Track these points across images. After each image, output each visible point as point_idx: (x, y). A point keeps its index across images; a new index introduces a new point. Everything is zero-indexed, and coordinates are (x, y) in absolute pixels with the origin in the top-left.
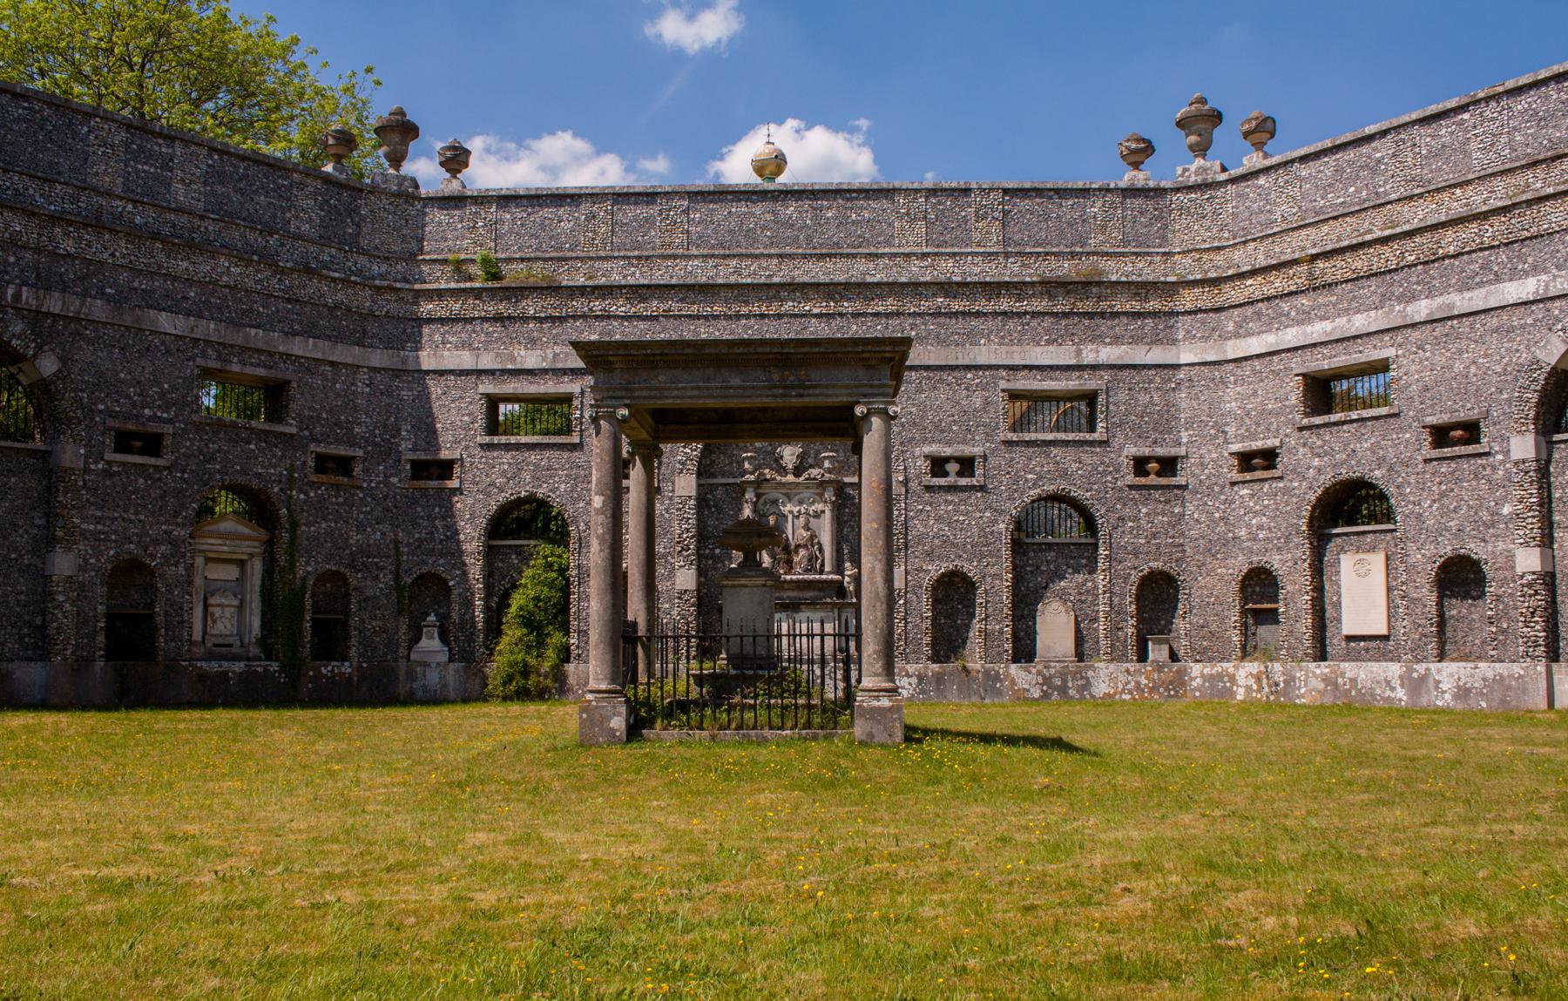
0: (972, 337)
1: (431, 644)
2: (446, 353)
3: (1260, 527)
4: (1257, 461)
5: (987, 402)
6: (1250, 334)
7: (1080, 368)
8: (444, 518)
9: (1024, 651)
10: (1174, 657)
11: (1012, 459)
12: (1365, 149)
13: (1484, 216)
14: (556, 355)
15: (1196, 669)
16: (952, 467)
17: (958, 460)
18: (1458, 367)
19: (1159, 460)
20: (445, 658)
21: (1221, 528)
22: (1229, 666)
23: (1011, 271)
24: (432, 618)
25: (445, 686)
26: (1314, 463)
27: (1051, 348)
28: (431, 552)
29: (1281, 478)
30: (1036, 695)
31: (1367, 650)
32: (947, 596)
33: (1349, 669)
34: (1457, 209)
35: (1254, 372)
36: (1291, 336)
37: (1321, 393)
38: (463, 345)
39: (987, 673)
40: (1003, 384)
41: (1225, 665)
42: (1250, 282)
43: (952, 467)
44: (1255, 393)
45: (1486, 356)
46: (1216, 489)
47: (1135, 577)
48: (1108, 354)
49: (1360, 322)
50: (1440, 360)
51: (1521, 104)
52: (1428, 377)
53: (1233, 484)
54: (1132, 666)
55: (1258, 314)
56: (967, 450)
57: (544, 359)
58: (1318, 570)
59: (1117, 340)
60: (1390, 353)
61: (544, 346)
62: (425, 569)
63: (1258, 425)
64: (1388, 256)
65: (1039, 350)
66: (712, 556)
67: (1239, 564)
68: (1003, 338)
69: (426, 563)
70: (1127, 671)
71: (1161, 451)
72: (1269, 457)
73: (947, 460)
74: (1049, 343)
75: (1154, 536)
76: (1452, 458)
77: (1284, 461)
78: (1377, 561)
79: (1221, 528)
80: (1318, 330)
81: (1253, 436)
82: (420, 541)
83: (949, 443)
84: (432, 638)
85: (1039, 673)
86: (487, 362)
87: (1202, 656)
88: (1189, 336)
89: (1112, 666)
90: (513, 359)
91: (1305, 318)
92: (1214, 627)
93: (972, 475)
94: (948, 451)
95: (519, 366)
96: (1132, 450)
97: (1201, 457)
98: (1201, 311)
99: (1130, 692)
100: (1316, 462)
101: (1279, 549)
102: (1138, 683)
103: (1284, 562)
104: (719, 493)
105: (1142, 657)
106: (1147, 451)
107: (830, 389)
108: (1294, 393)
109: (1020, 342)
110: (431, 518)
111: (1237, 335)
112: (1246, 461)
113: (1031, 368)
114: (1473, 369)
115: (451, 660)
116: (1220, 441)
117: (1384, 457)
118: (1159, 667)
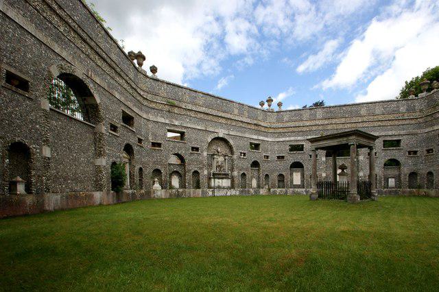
0: (245, 132)
4: (281, 158)
23: (249, 121)
26: (292, 158)
33: (296, 190)
34: (314, 124)
36: (287, 139)
38: (162, 117)
48: (261, 138)
49: (299, 138)
58: (291, 174)
64: (304, 129)
67: (277, 174)
72: (283, 157)
78: (299, 174)
80: (292, 138)
86: (167, 122)
91: (290, 136)
108: (288, 148)
112: (278, 157)
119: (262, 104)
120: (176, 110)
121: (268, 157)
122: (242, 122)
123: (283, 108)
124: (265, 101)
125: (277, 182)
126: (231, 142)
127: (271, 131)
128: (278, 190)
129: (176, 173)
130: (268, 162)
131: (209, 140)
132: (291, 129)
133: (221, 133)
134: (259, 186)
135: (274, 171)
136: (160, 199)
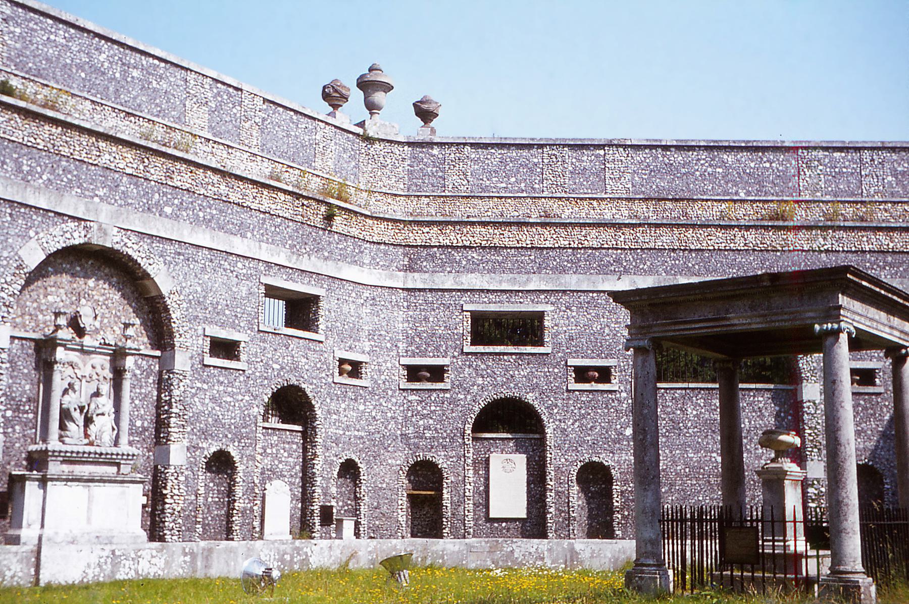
0: (241, 230)
6: (420, 271)
11: (265, 348)
12: (525, 153)
13: (618, 226)
18: (596, 327)
21: (392, 426)
31: (508, 530)
34: (594, 217)
37: (492, 329)
44: (426, 319)
45: (617, 323)
46: (390, 393)
50: (583, 321)
51: (640, 156)
52: (574, 330)
55: (433, 256)
60: (548, 308)
63: (428, 345)
64: (547, 238)
67: (400, 458)
72: (437, 373)
76: (590, 391)
77: (449, 376)
81: (423, 354)
88: (374, 264)
92: (384, 509)
100: (480, 381)
101: (444, 447)
107: (783, 315)
112: (414, 373)
114: (607, 331)
116: (394, 353)
117: (537, 385)
121: (355, 369)
122: (223, 174)
123: (444, 128)
124: (350, 83)
126: (163, 279)
130: (360, 394)
131: (33, 257)
132: (479, 236)
133: (110, 224)
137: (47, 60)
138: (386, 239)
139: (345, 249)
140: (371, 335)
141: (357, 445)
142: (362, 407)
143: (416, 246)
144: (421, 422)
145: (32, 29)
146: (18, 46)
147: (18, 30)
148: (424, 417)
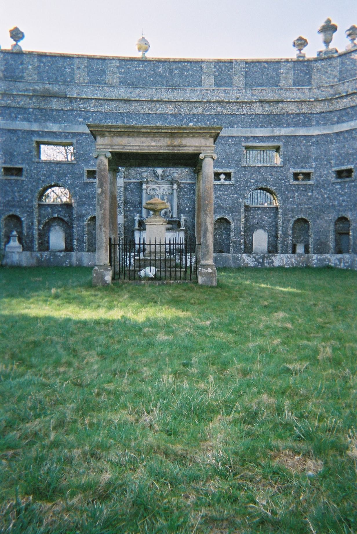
1: (14, 243)
2: (18, 122)
3: (343, 201)
5: (236, 151)
6: (343, 122)
7: (273, 137)
8: (19, 192)
9: (248, 250)
10: (307, 251)
14: (65, 127)
15: (315, 256)
16: (223, 177)
17: (225, 174)
19: (303, 174)
20: (21, 250)
21: (327, 201)
22: (328, 256)
24: (15, 233)
25: (21, 261)
27: (262, 129)
28: (13, 206)
29: (353, 181)
30: (252, 266)
32: (219, 227)
35: (344, 137)
39: (234, 257)
40: (243, 144)
41: (326, 255)
42: (345, 100)
43: (223, 177)
44: (344, 147)
47: (292, 220)
53: (333, 183)
54: (289, 255)
55: (348, 114)
56: (228, 171)
57: (60, 128)
59: (288, 125)
61: (60, 122)
62: (11, 213)
63: (344, 159)
65: (257, 129)
66: (129, 210)
68: (244, 125)
69: (11, 211)
70: (288, 257)
71: (304, 171)
73: (220, 174)
74: (262, 127)
75: (300, 204)
79: (327, 201)
81: (342, 164)
82: (9, 201)
83: (221, 167)
84: (14, 241)
85: (254, 257)
86: (35, 127)
87: (318, 251)
88: (318, 124)
89: (282, 255)
90: (47, 128)
93: (230, 180)
94: (221, 171)
95: (49, 130)
96: (292, 171)
97: (320, 173)
98: (323, 112)
99: (288, 265)
102: (292, 262)
103: (352, 215)
104: (132, 185)
105: (294, 252)
106: (298, 171)
109: (250, 127)
110: (13, 192)
111: (338, 122)
112: (340, 174)
113: (254, 137)
115: (23, 250)
116: (329, 166)
118: (300, 255)
119: (301, 43)
120: (55, 104)
121: (307, 176)
125: (332, 237)
127: (318, 108)
128: (332, 259)
129: (59, 219)
134: (273, 249)
135: (323, 209)
136: (17, 268)
137: (135, 78)
138: (324, 110)
139: (299, 120)
140: (316, 160)
141: (306, 212)
142: (309, 194)
143: (340, 110)
144: (341, 198)
145: (129, 68)
146: (123, 76)
147: (123, 70)
148: (342, 195)
